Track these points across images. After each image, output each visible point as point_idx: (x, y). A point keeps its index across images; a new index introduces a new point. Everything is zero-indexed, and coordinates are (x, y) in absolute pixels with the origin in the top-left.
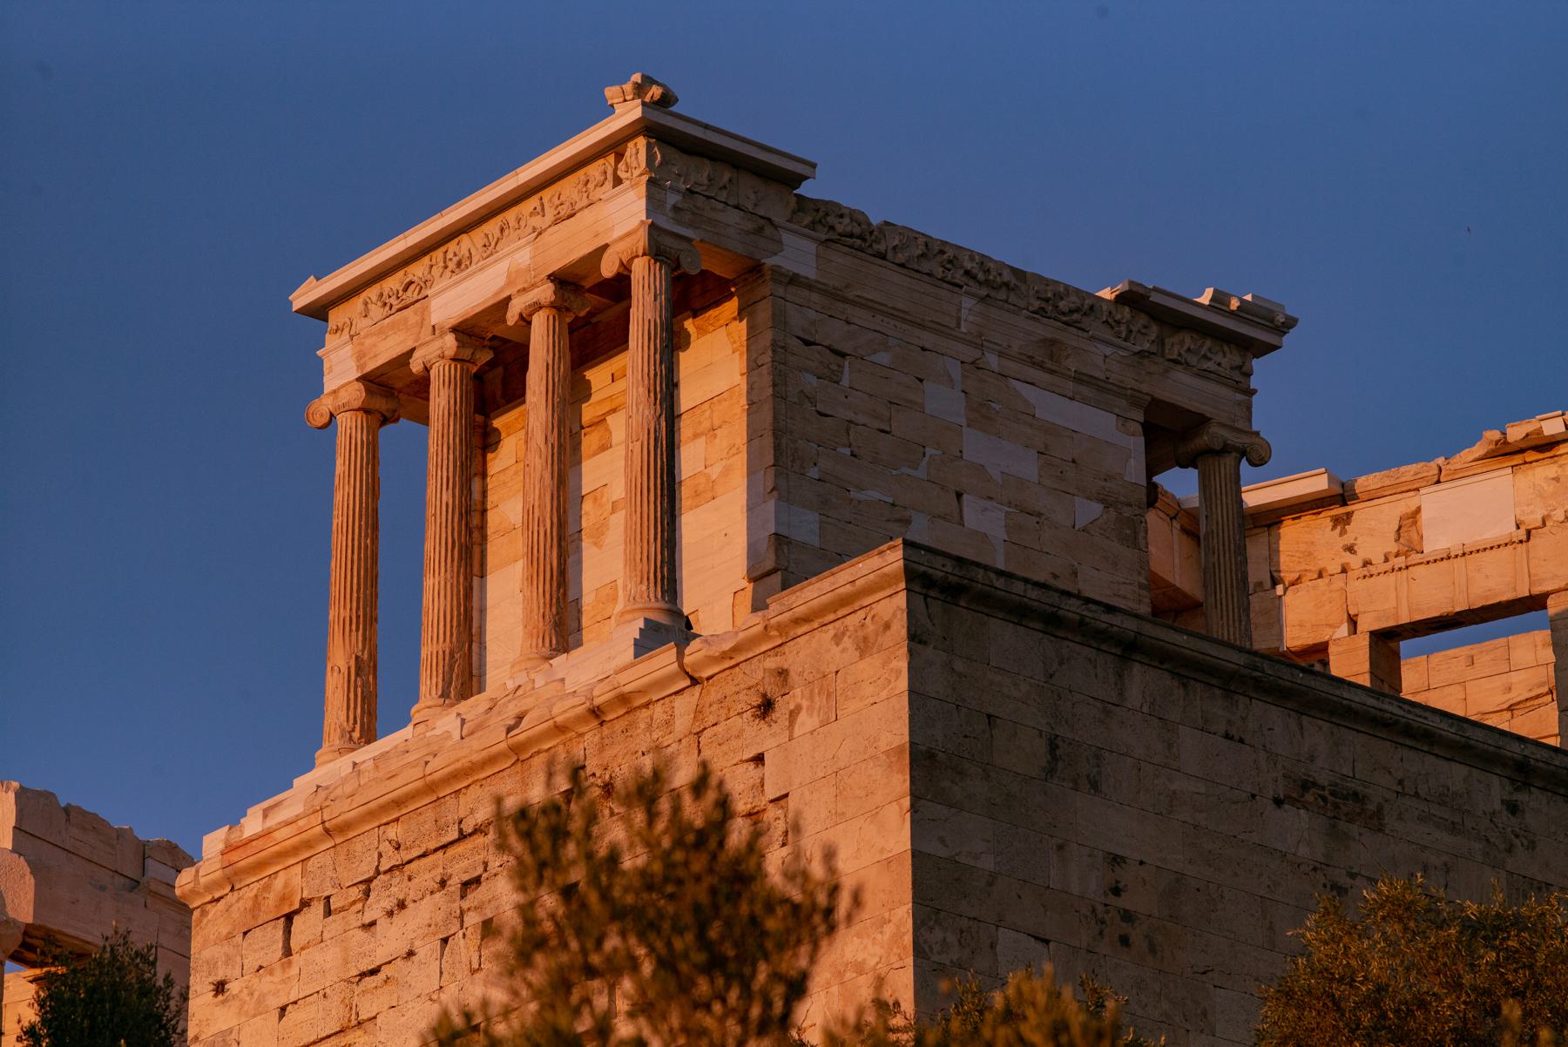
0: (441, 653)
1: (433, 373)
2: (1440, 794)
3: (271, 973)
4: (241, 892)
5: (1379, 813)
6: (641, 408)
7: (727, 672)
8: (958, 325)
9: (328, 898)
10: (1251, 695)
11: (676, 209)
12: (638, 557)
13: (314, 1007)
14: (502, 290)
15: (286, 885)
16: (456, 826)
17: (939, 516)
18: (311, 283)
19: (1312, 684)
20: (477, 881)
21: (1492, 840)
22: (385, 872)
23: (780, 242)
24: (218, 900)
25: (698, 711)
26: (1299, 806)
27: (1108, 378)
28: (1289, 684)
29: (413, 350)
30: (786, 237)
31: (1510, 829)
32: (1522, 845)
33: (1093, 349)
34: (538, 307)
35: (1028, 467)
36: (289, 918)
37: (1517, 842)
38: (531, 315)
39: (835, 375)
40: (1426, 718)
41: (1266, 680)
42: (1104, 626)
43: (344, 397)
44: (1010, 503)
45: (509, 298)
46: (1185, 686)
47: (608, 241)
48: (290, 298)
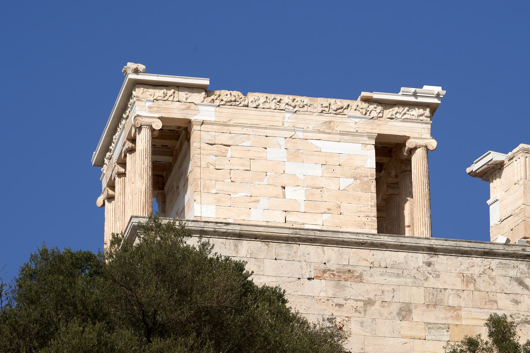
2: (392, 265)
5: (360, 276)
8: (283, 124)
10: (299, 243)
11: (150, 107)
17: (273, 197)
19: (324, 235)
21: (417, 277)
23: (198, 110)
26: (321, 278)
27: (357, 131)
28: (313, 237)
30: (200, 107)
31: (427, 272)
32: (433, 277)
33: (349, 121)
35: (318, 171)
37: (431, 276)
39: (224, 154)
40: (380, 239)
41: (302, 237)
42: (226, 230)
44: (308, 186)
46: (267, 245)
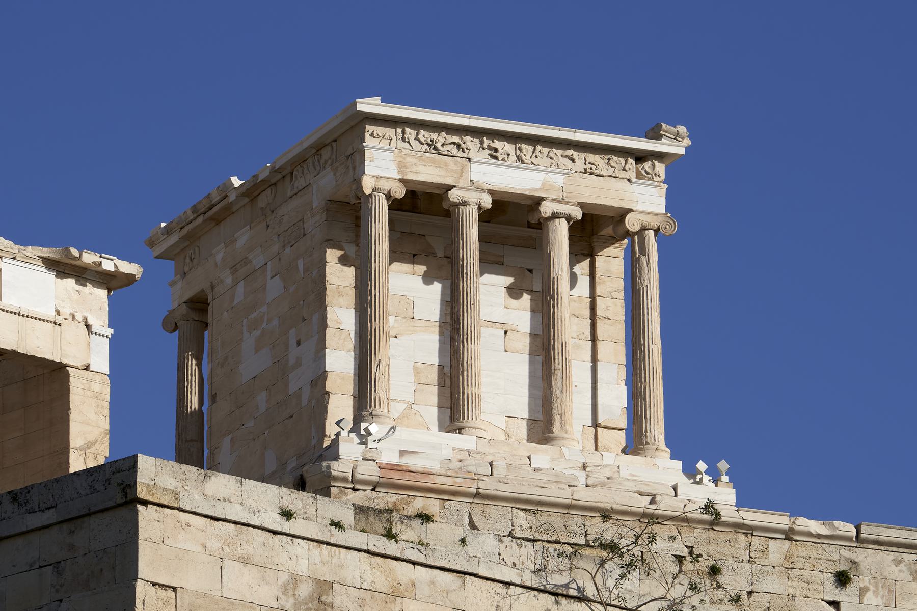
4: (380, 495)
7: (811, 544)
14: (537, 190)
29: (455, 187)
43: (386, 186)
48: (357, 100)
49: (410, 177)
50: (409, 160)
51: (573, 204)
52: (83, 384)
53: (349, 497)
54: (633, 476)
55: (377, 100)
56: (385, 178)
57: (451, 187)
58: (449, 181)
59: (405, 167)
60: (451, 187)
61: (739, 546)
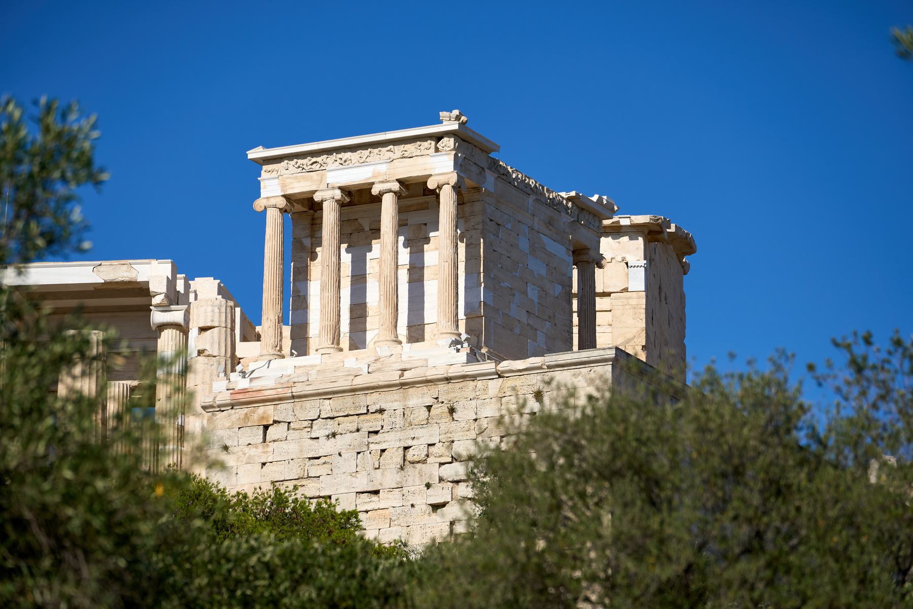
0: (331, 325)
1: (325, 205)
3: (256, 448)
6: (448, 249)
7: (517, 377)
9: (289, 423)
12: (447, 311)
13: (283, 467)
14: (369, 178)
15: (264, 413)
16: (366, 408)
18: (260, 148)
20: (376, 432)
22: (323, 419)
24: (223, 411)
25: (501, 388)
29: (317, 191)
34: (390, 191)
35: (543, 271)
36: (266, 427)
38: (384, 193)
43: (273, 202)
45: (373, 183)
47: (432, 174)
48: (247, 152)
49: (289, 192)
50: (288, 181)
51: (393, 181)
52: (622, 302)
53: (217, 417)
54: (410, 357)
55: (260, 148)
56: (272, 197)
57: (314, 192)
58: (314, 188)
59: (286, 186)
60: (314, 192)
61: (468, 390)
